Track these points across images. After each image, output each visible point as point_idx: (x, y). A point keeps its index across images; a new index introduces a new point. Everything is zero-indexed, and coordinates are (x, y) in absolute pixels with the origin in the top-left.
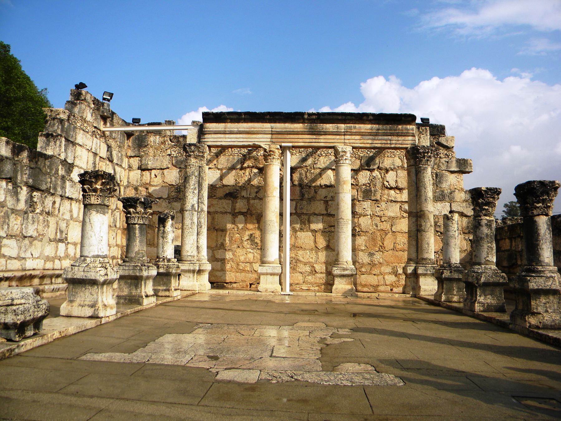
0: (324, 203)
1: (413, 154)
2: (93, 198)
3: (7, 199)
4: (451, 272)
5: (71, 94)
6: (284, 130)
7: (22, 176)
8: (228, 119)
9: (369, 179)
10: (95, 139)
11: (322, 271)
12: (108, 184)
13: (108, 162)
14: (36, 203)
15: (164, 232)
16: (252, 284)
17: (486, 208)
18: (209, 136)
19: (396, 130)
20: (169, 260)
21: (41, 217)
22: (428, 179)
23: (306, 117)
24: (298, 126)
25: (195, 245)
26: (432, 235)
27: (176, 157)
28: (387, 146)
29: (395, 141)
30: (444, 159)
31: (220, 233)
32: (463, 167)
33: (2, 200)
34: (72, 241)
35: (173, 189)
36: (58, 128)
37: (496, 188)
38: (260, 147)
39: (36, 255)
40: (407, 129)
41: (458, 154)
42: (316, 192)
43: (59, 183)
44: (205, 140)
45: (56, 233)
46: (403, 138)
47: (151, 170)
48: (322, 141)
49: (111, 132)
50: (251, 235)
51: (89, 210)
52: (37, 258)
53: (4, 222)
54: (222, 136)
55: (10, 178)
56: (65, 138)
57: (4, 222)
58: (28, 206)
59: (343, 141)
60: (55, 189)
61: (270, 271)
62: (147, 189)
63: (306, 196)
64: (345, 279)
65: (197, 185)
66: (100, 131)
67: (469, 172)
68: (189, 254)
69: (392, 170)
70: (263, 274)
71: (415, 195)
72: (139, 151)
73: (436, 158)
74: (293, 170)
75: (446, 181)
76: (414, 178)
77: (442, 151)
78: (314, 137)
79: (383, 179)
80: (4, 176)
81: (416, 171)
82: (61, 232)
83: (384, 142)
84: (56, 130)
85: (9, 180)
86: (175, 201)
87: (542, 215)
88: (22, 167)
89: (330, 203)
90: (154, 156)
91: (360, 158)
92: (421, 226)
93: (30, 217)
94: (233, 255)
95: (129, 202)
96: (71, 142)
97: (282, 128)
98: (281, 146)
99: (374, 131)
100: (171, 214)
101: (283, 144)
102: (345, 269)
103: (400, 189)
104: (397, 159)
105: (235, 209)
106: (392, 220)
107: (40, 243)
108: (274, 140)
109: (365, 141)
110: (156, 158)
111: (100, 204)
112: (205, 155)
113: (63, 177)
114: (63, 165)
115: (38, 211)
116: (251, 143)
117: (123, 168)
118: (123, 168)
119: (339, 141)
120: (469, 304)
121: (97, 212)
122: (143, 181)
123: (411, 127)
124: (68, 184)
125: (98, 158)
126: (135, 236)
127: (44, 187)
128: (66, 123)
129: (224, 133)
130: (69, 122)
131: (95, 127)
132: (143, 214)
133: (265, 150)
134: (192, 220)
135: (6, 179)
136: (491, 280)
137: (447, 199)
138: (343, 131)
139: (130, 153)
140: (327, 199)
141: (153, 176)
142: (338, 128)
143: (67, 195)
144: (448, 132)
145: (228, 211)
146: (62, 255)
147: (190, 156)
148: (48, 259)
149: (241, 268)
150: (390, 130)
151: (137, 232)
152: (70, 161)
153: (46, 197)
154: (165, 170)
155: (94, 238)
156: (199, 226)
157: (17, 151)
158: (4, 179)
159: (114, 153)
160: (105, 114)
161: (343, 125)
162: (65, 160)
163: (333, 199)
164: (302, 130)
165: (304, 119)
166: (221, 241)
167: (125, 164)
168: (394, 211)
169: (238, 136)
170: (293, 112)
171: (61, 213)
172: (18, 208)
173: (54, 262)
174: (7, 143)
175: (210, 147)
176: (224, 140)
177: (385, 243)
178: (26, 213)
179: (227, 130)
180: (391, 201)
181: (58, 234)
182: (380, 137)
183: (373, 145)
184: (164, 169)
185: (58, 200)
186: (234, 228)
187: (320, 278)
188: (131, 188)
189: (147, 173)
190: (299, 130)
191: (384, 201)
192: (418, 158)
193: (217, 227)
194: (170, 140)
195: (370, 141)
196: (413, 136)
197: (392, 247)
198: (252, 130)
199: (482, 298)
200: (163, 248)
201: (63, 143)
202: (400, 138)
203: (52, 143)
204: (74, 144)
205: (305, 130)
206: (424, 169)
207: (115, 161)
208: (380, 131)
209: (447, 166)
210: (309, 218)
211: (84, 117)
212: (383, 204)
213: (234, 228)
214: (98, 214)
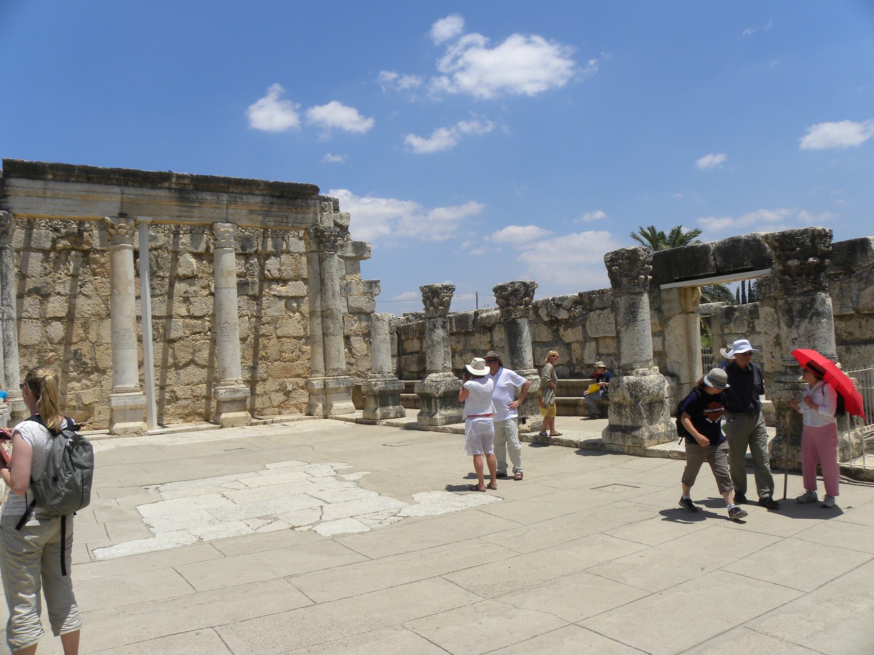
1: (316, 237)
4: (386, 384)
8: (48, 173)
11: (186, 396)
23: (174, 180)
61: (130, 402)
64: (236, 405)
67: (365, 259)
76: (317, 267)
83: (279, 219)
92: (328, 328)
101: (140, 219)
102: (236, 391)
103: (284, 281)
136: (452, 388)
142: (218, 197)
161: (225, 195)
169: (68, 202)
180: (274, 296)
186: (45, 343)
187: (184, 407)
192: (321, 242)
195: (260, 218)
213: (45, 343)
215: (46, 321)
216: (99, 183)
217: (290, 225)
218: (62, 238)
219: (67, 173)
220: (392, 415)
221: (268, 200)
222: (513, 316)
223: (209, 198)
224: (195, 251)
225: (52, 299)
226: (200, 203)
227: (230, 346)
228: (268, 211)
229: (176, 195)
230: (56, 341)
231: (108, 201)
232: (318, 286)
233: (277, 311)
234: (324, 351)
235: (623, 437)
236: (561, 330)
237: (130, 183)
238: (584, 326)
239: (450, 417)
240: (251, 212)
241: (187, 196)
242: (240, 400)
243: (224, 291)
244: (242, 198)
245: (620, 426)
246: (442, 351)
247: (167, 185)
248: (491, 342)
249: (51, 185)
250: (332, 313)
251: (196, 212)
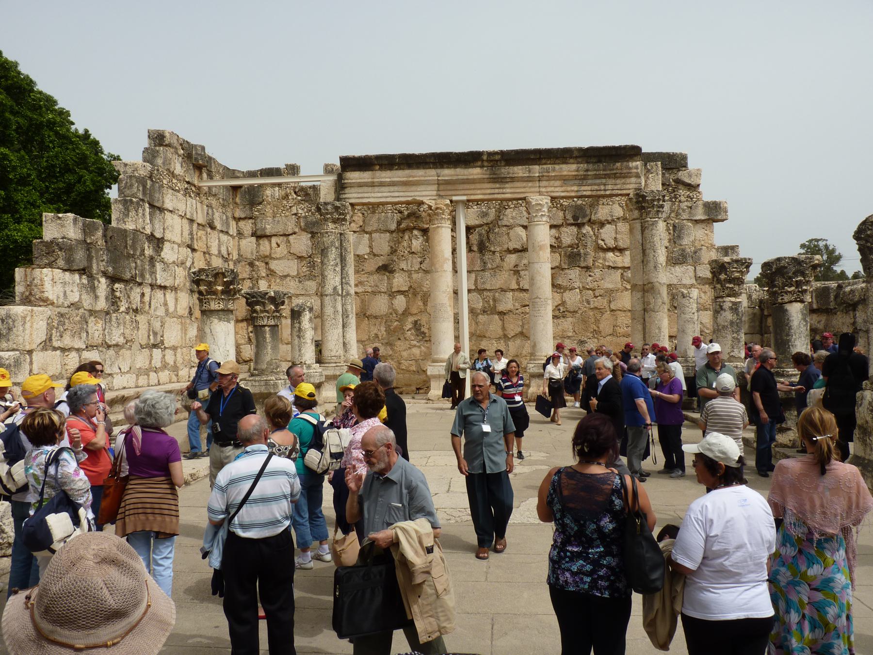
0: (514, 274)
1: (637, 202)
2: (212, 304)
3: (83, 297)
5: (149, 137)
6: (455, 178)
7: (98, 264)
9: (577, 238)
10: (189, 200)
12: (231, 282)
13: (209, 230)
14: (119, 298)
15: (300, 328)
17: (731, 286)
18: (353, 190)
19: (613, 170)
20: (309, 367)
21: (128, 317)
22: (658, 238)
23: (485, 157)
24: (475, 172)
25: (341, 340)
26: (665, 316)
27: (306, 217)
28: (599, 193)
29: (611, 186)
30: (686, 203)
31: (374, 320)
32: (714, 213)
33: (77, 300)
34: (171, 344)
36: (138, 190)
37: (745, 259)
38: (422, 203)
39: (125, 369)
41: (708, 193)
42: (502, 260)
43: (147, 267)
44: (346, 196)
45: (149, 336)
46: (623, 180)
47: (270, 236)
48: (508, 190)
49: (210, 188)
50: (416, 322)
51: (208, 317)
52: (128, 372)
53: (82, 328)
55: (84, 270)
56: (149, 204)
57: (82, 328)
58: (109, 304)
59: (537, 189)
60: (142, 276)
62: (267, 263)
63: (489, 266)
65: (338, 260)
66: (195, 186)
67: (723, 221)
68: (333, 354)
69: (609, 223)
71: (640, 260)
72: (251, 209)
73: (673, 203)
74: (469, 229)
75: (689, 234)
76: (639, 237)
77: (683, 192)
78: (498, 186)
79: (597, 237)
80: (75, 268)
81: (642, 227)
82: (155, 334)
83: (596, 187)
84: (136, 193)
85: (83, 271)
87: (796, 301)
88: (97, 251)
89: (522, 273)
90: (274, 217)
91: (563, 209)
92: (649, 303)
93: (114, 319)
95: (253, 297)
96: (157, 209)
97: (451, 176)
98: (451, 201)
99: (582, 173)
100: (308, 304)
101: (454, 198)
103: (621, 250)
104: (616, 206)
105: (391, 288)
106: (610, 293)
107: (128, 352)
108: (442, 193)
109: (569, 189)
110: (276, 219)
111: (222, 310)
112: (348, 217)
113: (152, 259)
114: (149, 242)
115: (122, 309)
116: (409, 199)
117: (231, 236)
118: (231, 236)
119: (532, 190)
121: (220, 319)
122: (261, 253)
123: (636, 164)
124: (159, 266)
125: (195, 226)
126: (265, 341)
127: (128, 276)
128: (149, 182)
129: (372, 185)
130: (152, 181)
131: (188, 183)
132: (274, 312)
133: (430, 207)
134: (335, 307)
135: (78, 270)
137: (690, 260)
138: (537, 175)
139: (238, 213)
140: (519, 269)
141: (274, 245)
142: (530, 171)
143: (159, 282)
144: (692, 165)
145: (383, 290)
146: (159, 365)
147: (326, 220)
148: (140, 372)
150: (604, 170)
151: (268, 336)
152: (158, 235)
153: (131, 288)
154: (291, 237)
155: (218, 352)
156: (345, 315)
157: (87, 230)
158: (75, 270)
159: (217, 215)
160: (200, 162)
161: (537, 167)
162: (152, 235)
163: (527, 267)
164: (480, 176)
165: (483, 161)
166: (375, 332)
167: (233, 231)
168: (613, 280)
169: (392, 189)
171: (153, 307)
172: (98, 309)
173: (148, 376)
174: (75, 220)
175: (352, 205)
176: (373, 195)
177: (601, 326)
178: (108, 313)
179: (376, 180)
181: (151, 337)
182: (590, 182)
183: (580, 194)
184: (289, 235)
185: (147, 290)
186: (391, 314)
188: (243, 263)
189: (265, 243)
190: (475, 177)
191: (598, 267)
192: (643, 208)
193: (368, 313)
194: (295, 193)
195: (575, 188)
196: (638, 176)
197: (611, 331)
198: (411, 179)
200: (300, 350)
201: (148, 210)
202: (618, 181)
203: (132, 213)
204: (161, 210)
205: (485, 176)
206: (653, 224)
207: (219, 226)
208: (589, 173)
209: (690, 213)
210: (494, 296)
211: (172, 170)
212: (597, 272)
214: (221, 323)
215: (392, 295)
216: (418, 168)
218: (405, 219)
222: (780, 301)
224: (525, 224)
225: (397, 275)
227: (541, 321)
230: (400, 312)
232: (639, 257)
234: (644, 329)
243: (536, 265)
246: (729, 337)
247: (479, 163)
248: (854, 323)
250: (653, 288)
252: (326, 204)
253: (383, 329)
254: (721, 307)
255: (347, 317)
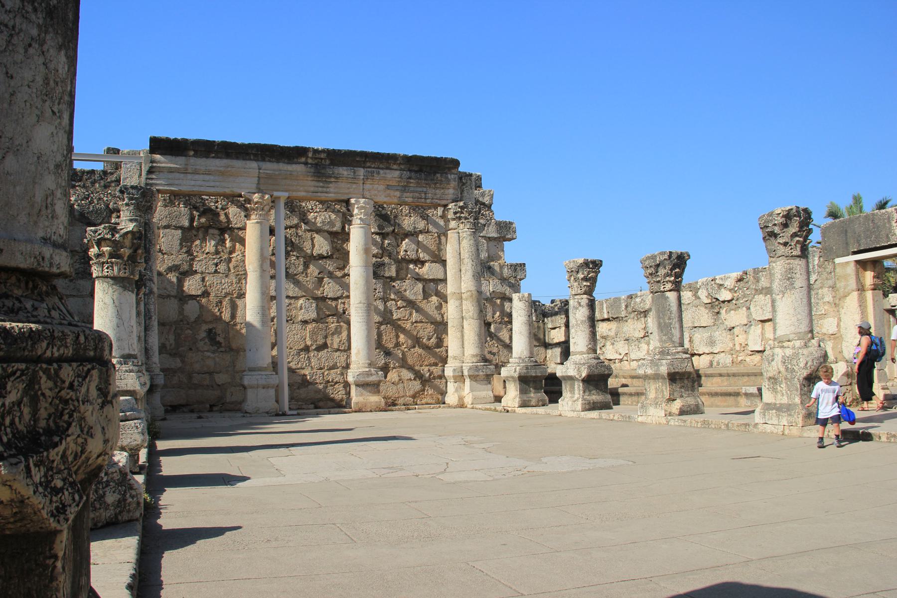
1: (455, 213)
2: (116, 268)
4: (527, 368)
8: (189, 150)
16: (214, 405)
23: (310, 155)
35: (77, 257)
40: (447, 178)
48: (332, 190)
50: (210, 331)
54: (182, 175)
61: (262, 382)
64: (369, 388)
67: (510, 240)
70: (252, 387)
78: (321, 184)
83: (417, 195)
86: (82, 278)
94: (183, 362)
101: (276, 194)
120: (570, 403)
136: (596, 372)
142: (354, 173)
149: (196, 382)
165: (307, 157)
169: (207, 177)
170: (292, 146)
195: (398, 194)
199: (587, 394)
214: (126, 292)
216: (237, 158)
217: (428, 201)
219: (205, 148)
220: (533, 403)
221: (406, 174)
223: (345, 173)
224: (331, 230)
226: (337, 178)
228: (405, 186)
229: (312, 170)
231: (245, 177)
233: (415, 294)
235: (778, 416)
236: (723, 311)
237: (267, 159)
238: (748, 308)
239: (594, 403)
240: (388, 187)
241: (323, 171)
242: (374, 384)
244: (378, 173)
245: (775, 404)
247: (303, 160)
248: (645, 328)
249: (193, 160)
251: (332, 188)
252: (132, 187)
253: (172, 337)
254: (579, 303)
255: (150, 318)
